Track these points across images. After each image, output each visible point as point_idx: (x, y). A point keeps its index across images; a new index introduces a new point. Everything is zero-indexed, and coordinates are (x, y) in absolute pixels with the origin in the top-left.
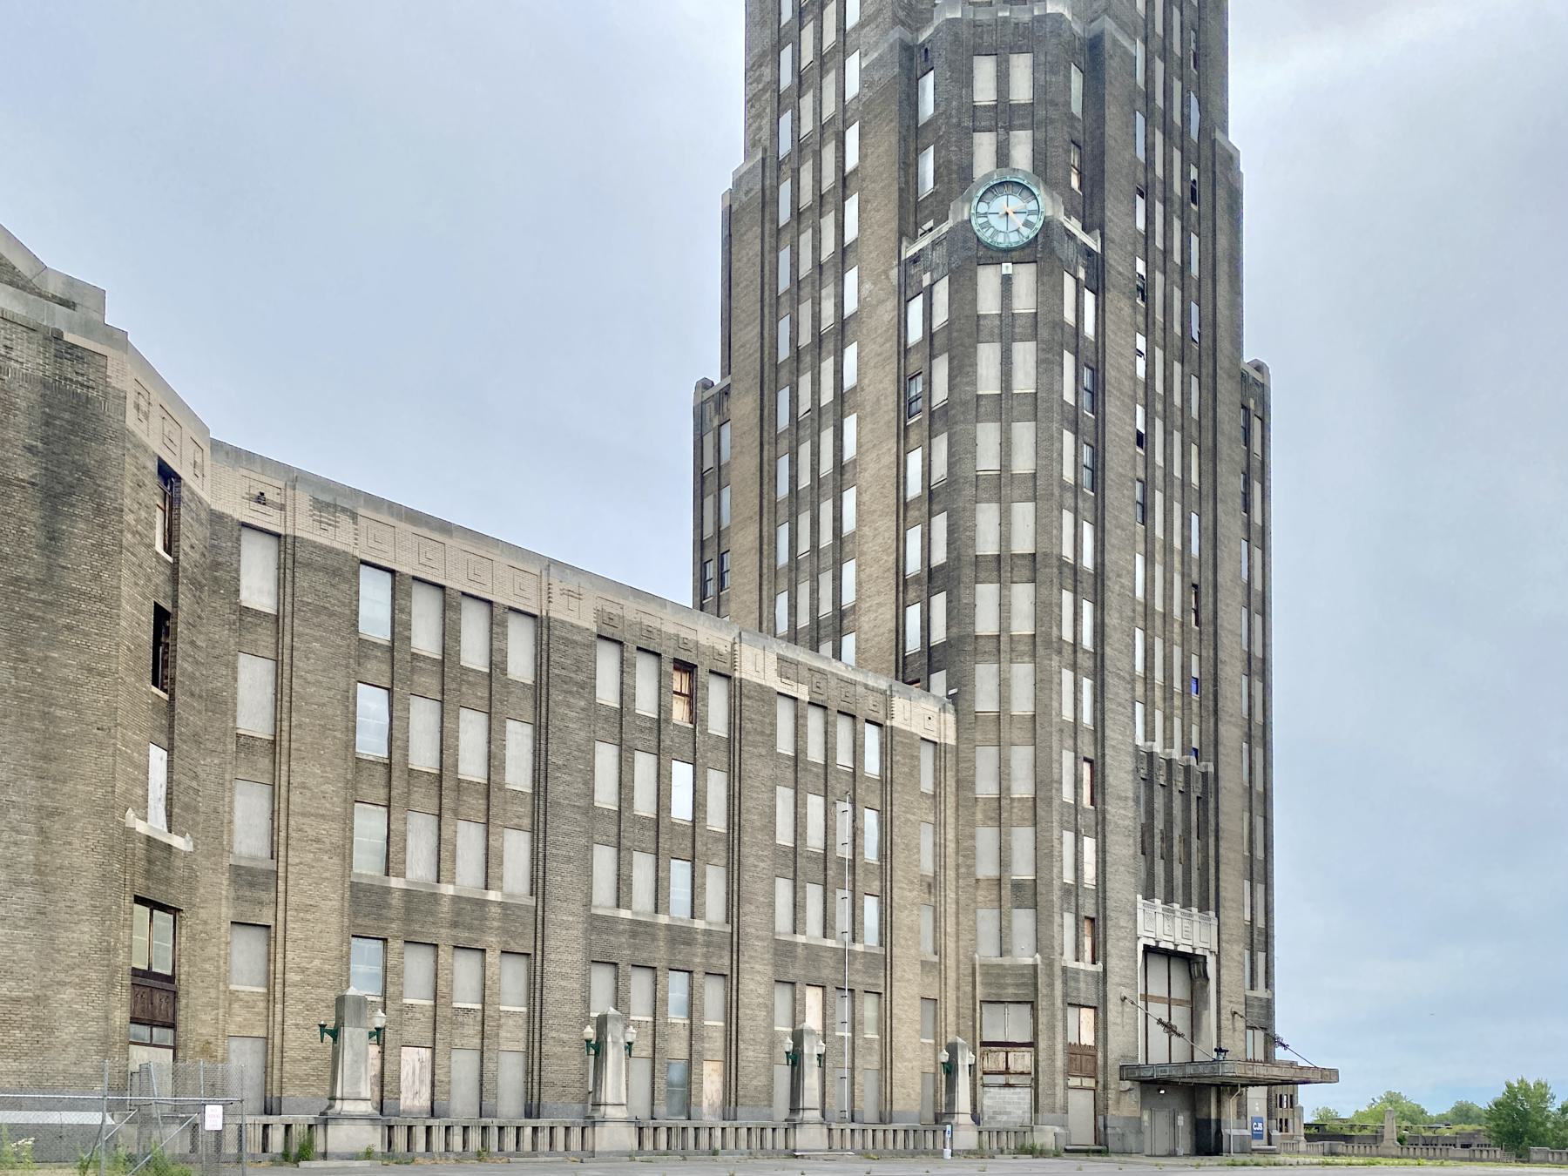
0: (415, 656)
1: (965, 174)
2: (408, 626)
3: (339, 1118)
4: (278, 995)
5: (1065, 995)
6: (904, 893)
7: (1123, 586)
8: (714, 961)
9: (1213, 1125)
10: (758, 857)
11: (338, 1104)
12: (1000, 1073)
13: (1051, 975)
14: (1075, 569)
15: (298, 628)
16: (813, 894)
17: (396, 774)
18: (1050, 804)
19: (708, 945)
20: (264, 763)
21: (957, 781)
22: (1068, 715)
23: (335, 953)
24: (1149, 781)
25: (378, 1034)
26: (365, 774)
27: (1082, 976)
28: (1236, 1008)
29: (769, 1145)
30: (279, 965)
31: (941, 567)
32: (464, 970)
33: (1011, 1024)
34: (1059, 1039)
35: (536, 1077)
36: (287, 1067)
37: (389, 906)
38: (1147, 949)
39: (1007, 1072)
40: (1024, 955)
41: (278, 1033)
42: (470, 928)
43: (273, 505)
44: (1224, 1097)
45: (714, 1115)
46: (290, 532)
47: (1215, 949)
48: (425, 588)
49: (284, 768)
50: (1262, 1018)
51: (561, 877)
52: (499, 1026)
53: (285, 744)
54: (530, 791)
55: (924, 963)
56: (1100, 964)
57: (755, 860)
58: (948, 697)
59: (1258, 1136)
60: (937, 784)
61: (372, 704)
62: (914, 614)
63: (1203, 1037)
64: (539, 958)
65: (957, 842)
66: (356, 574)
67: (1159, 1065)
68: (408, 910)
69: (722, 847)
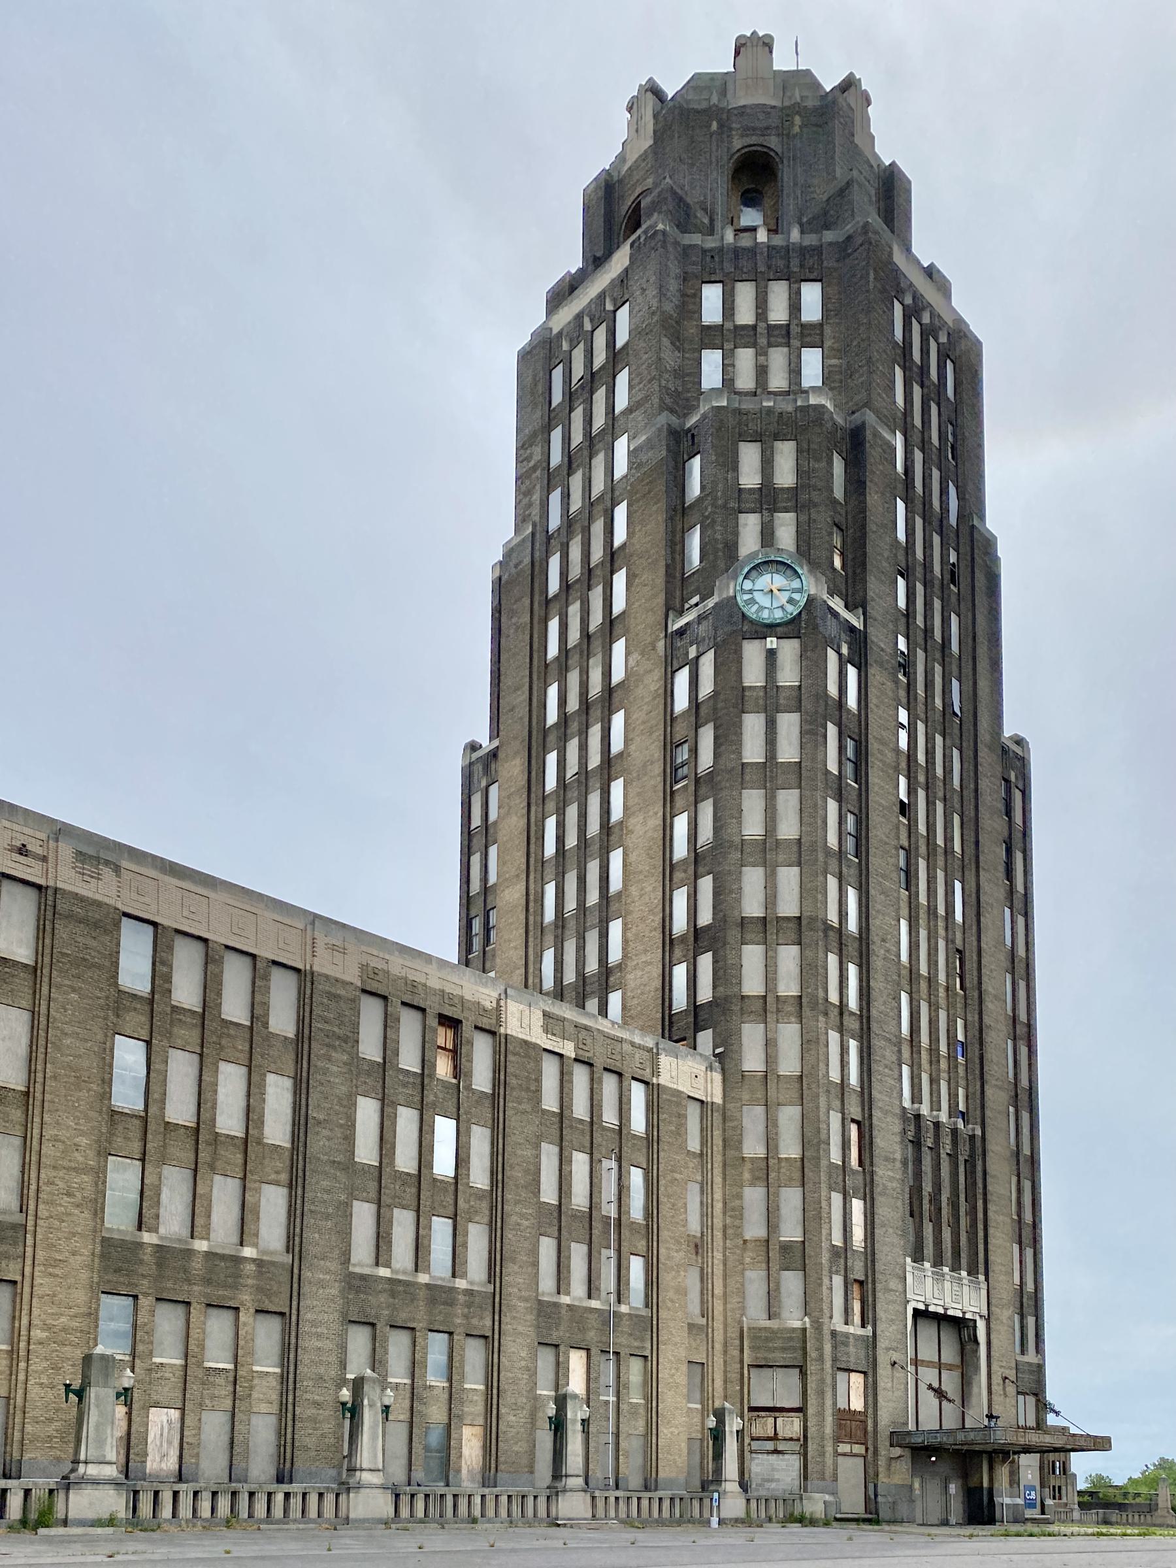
0: (176, 1009)
1: (731, 548)
2: (168, 979)
3: (85, 1481)
4: (22, 1353)
5: (835, 1360)
6: (672, 1253)
7: (888, 951)
8: (475, 1321)
9: (985, 1492)
10: (522, 1216)
11: (81, 1468)
12: (769, 1439)
13: (820, 1339)
14: (841, 931)
15: (57, 979)
16: (578, 1253)
17: (152, 1127)
18: (818, 1165)
19: (469, 1305)
20: (17, 1114)
21: (724, 1140)
22: (835, 1076)
23: (84, 1310)
24: (917, 1143)
25: (125, 1394)
26: (120, 1128)
27: (851, 1340)
28: (1007, 1373)
29: (530, 1512)
30: (25, 1321)
31: (708, 927)
32: (217, 1327)
33: (777, 1388)
34: (829, 1402)
35: (289, 1440)
36: (28, 1428)
37: (141, 1262)
38: (916, 1312)
39: (775, 1438)
40: (794, 1319)
41: (20, 1392)
42: (225, 1286)
43: (36, 857)
44: (997, 1466)
45: (473, 1481)
46: (51, 883)
47: (985, 1313)
48: (188, 940)
49: (37, 1120)
50: (1033, 1384)
51: (316, 1239)
52: (251, 1388)
53: (38, 1095)
54: (288, 1145)
55: (691, 1326)
56: (870, 1328)
57: (518, 1215)
58: (715, 1055)
59: (1030, 1504)
60: (704, 1143)
61: (129, 1056)
62: (680, 973)
63: (974, 1400)
64: (294, 1318)
65: (725, 1203)
66: (117, 925)
67: (930, 1432)
68: (160, 1265)
69: (485, 1205)
